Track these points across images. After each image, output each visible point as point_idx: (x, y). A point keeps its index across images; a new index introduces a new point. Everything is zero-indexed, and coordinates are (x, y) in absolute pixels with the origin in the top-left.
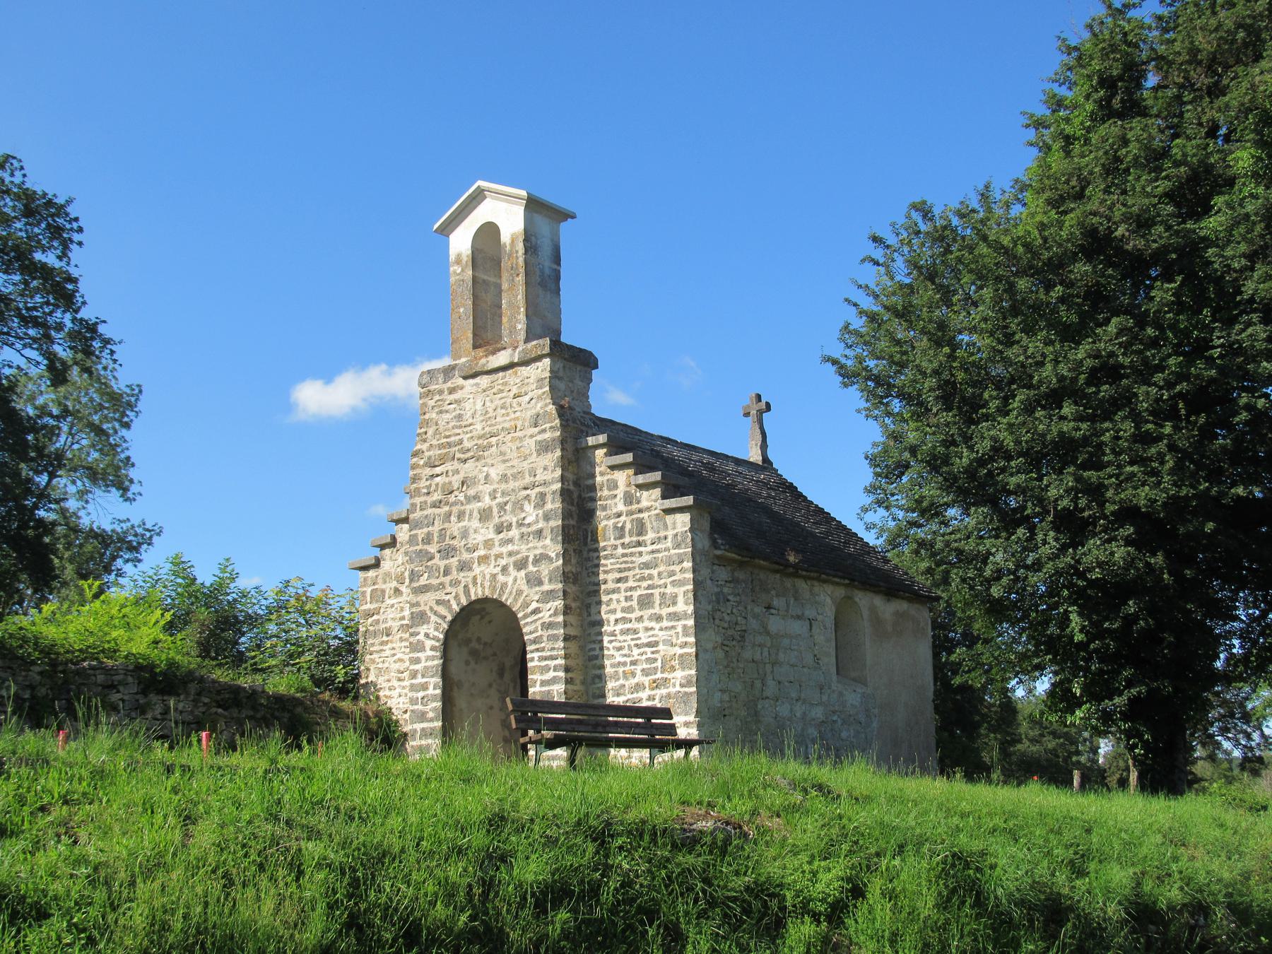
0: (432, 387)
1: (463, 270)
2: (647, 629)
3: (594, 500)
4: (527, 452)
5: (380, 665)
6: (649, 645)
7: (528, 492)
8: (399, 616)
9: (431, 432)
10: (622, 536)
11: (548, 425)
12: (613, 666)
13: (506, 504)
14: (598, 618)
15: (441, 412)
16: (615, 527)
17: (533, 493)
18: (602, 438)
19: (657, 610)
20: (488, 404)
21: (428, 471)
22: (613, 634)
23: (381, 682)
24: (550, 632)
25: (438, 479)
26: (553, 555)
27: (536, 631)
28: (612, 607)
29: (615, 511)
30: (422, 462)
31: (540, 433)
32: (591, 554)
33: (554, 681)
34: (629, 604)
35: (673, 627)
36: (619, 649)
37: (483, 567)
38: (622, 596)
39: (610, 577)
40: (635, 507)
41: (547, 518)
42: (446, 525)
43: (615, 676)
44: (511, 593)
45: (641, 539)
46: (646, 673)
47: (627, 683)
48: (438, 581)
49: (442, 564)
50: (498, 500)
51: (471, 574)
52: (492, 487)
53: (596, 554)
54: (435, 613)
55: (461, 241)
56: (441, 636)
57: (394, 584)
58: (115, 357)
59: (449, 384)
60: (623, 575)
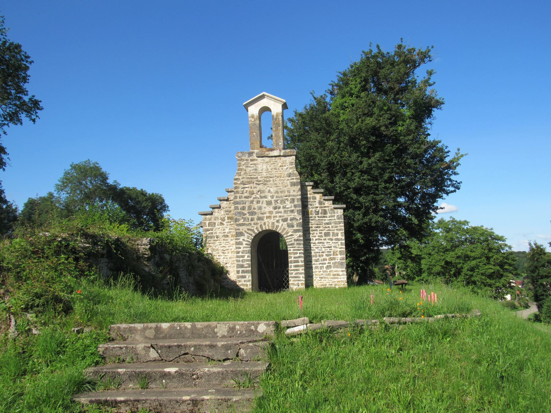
0: (243, 158)
1: (255, 120)
2: (327, 243)
3: (307, 202)
4: (286, 185)
5: (214, 248)
6: (328, 247)
7: (287, 197)
8: (222, 232)
9: (243, 173)
10: (318, 214)
11: (295, 177)
12: (314, 253)
13: (278, 200)
14: (309, 238)
15: (247, 167)
16: (315, 211)
17: (289, 198)
18: (311, 183)
19: (331, 237)
20: (268, 167)
21: (242, 186)
22: (315, 243)
23: (214, 253)
24: (297, 242)
25: (247, 189)
26: (298, 218)
27: (291, 241)
28: (314, 235)
29: (315, 206)
30: (239, 182)
31: (291, 179)
32: (306, 218)
33: (299, 257)
34: (321, 235)
35: (337, 243)
36: (317, 248)
37: (268, 220)
38: (318, 232)
39: (313, 226)
40: (323, 206)
41: (295, 206)
42: (252, 205)
43: (316, 256)
44: (281, 229)
45: (325, 215)
46: (327, 255)
47: (320, 258)
48: (248, 223)
49: (250, 217)
50: (274, 199)
51: (263, 222)
52: (272, 194)
53: (308, 219)
54: (247, 233)
55: (254, 110)
56: (251, 241)
57: (220, 221)
58: (37, 114)
59: (251, 158)
60: (318, 226)
